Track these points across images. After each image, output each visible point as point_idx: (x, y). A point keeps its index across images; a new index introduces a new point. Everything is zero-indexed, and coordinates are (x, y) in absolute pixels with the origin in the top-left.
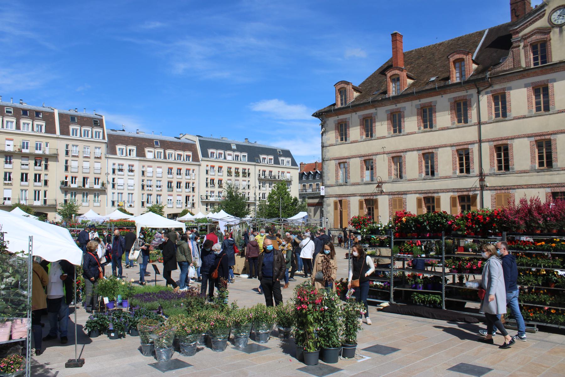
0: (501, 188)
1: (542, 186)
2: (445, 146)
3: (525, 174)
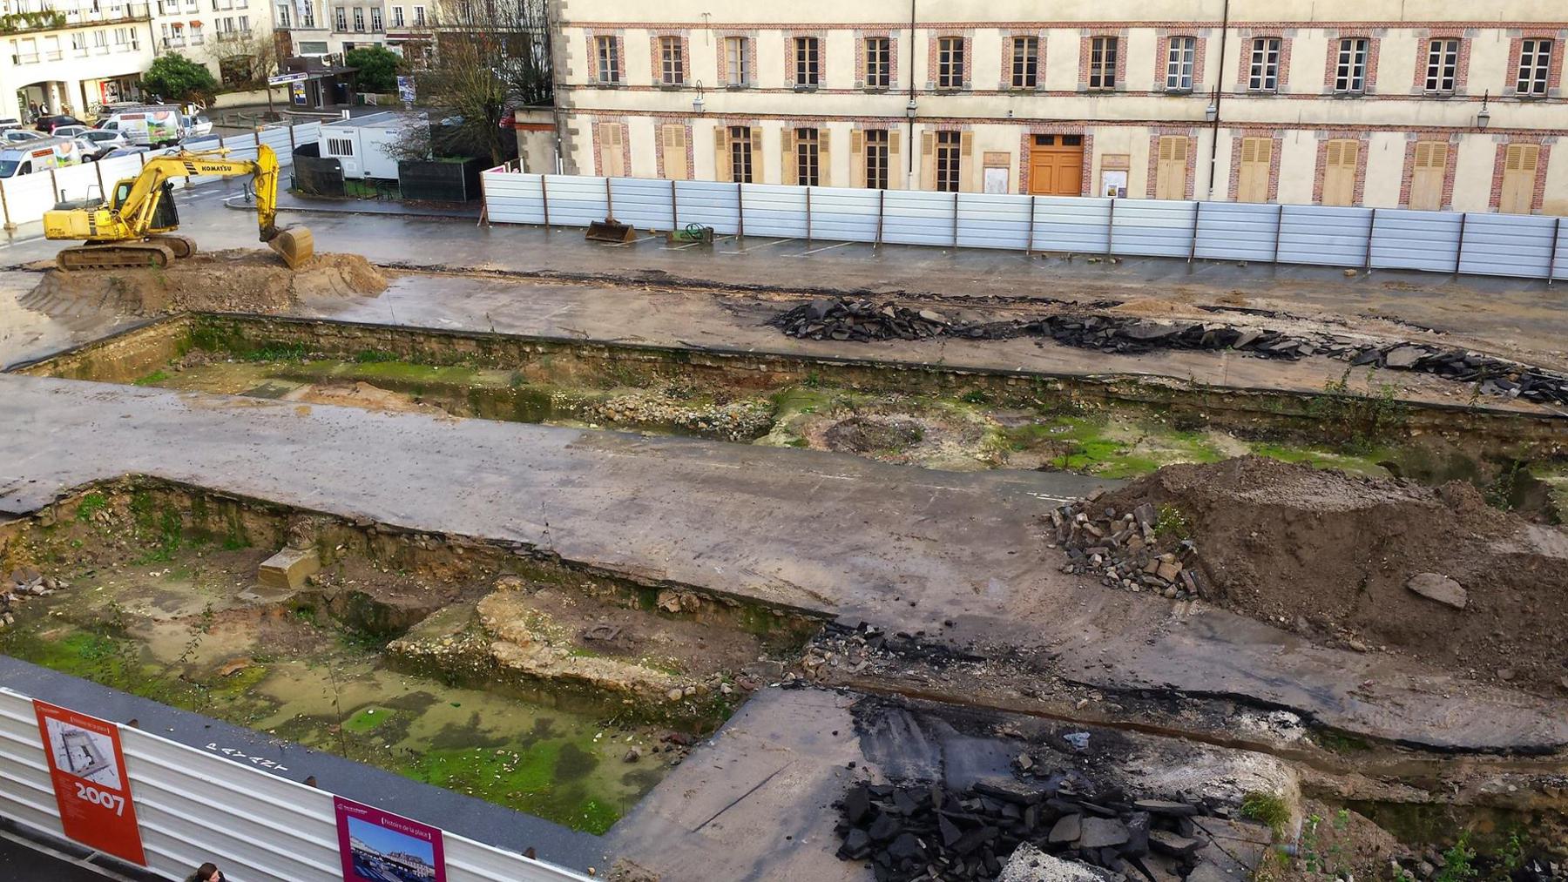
2: (841, 26)
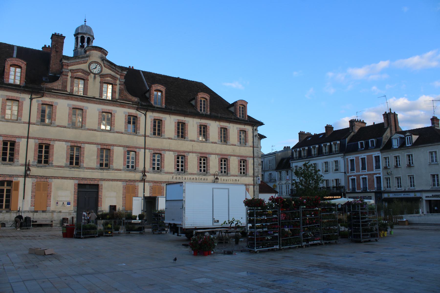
0: (42, 177)
1: (72, 178)
3: (61, 169)
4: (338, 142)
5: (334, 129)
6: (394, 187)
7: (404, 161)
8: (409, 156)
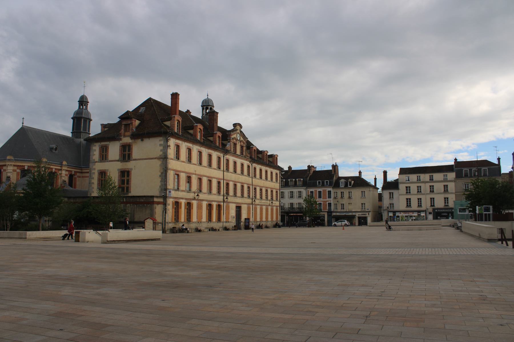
4: (302, 179)
5: (292, 169)
6: (339, 210)
7: (346, 195)
8: (349, 192)
